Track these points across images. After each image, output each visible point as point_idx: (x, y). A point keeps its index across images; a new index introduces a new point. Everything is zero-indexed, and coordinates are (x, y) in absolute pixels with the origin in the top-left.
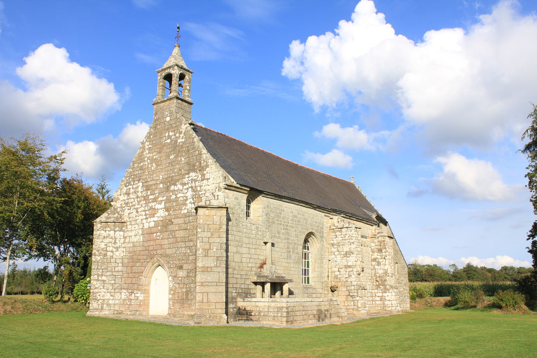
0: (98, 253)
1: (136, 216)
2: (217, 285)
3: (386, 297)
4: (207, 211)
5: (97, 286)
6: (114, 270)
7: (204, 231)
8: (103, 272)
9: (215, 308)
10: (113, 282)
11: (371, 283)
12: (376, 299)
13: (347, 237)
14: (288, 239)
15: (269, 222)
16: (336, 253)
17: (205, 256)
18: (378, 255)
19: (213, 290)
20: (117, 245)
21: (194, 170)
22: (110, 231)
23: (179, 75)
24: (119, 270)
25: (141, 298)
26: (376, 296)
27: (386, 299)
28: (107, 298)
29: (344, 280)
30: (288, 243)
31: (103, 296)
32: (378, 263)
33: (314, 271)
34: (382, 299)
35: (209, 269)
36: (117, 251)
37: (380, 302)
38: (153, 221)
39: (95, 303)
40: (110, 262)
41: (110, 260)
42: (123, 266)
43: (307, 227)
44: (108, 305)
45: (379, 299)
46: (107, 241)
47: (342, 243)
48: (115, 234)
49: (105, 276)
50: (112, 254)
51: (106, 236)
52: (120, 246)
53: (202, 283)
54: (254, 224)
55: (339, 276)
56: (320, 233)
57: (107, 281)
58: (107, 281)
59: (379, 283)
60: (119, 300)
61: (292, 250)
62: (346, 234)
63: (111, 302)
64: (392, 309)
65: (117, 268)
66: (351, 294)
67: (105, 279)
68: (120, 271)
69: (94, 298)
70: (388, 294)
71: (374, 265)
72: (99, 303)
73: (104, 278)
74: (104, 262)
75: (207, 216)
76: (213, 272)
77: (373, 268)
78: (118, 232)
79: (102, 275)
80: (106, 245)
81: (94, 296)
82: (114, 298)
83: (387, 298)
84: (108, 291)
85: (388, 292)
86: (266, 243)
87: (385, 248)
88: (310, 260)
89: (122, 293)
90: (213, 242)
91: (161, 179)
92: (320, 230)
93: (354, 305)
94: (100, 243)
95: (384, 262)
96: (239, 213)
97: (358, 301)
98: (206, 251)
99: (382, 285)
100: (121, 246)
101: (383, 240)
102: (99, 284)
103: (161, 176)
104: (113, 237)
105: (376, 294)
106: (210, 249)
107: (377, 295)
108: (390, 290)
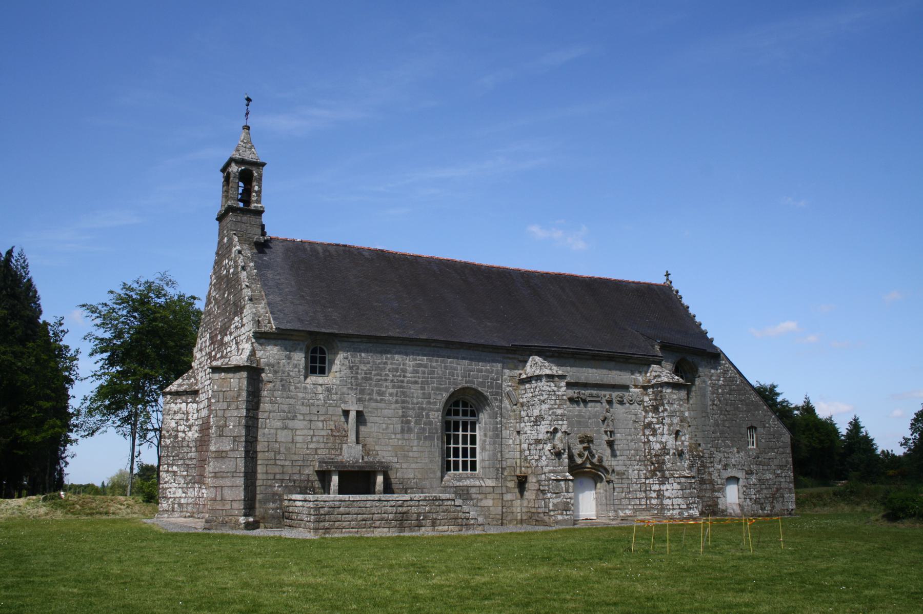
2: (233, 477)
3: (665, 492)
5: (167, 480)
7: (219, 402)
8: (173, 460)
9: (231, 509)
10: (185, 473)
12: (651, 495)
14: (403, 402)
15: (356, 378)
16: (526, 418)
17: (220, 436)
18: (653, 417)
19: (229, 484)
20: (190, 422)
22: (180, 403)
23: (237, 174)
24: (193, 457)
25: (205, 495)
26: (651, 490)
27: (665, 494)
28: (178, 496)
29: (535, 464)
32: (653, 432)
33: (483, 449)
34: (660, 495)
35: (224, 454)
36: (190, 430)
37: (656, 500)
40: (182, 446)
42: (196, 452)
43: (454, 379)
44: (180, 505)
45: (654, 495)
46: (177, 418)
49: (176, 465)
50: (184, 435)
53: (215, 473)
54: (321, 385)
55: (529, 458)
59: (655, 466)
60: (192, 498)
61: (413, 420)
62: (536, 387)
63: (183, 501)
64: (672, 515)
65: (190, 454)
66: (542, 488)
70: (667, 486)
71: (649, 435)
72: (170, 503)
73: (175, 468)
77: (646, 440)
79: (172, 465)
80: (177, 423)
83: (667, 494)
85: (667, 483)
86: (318, 412)
87: (663, 405)
88: (477, 433)
90: (229, 415)
92: (492, 383)
93: (545, 507)
95: (661, 429)
97: (549, 499)
99: (659, 471)
103: (219, 324)
107: (653, 489)
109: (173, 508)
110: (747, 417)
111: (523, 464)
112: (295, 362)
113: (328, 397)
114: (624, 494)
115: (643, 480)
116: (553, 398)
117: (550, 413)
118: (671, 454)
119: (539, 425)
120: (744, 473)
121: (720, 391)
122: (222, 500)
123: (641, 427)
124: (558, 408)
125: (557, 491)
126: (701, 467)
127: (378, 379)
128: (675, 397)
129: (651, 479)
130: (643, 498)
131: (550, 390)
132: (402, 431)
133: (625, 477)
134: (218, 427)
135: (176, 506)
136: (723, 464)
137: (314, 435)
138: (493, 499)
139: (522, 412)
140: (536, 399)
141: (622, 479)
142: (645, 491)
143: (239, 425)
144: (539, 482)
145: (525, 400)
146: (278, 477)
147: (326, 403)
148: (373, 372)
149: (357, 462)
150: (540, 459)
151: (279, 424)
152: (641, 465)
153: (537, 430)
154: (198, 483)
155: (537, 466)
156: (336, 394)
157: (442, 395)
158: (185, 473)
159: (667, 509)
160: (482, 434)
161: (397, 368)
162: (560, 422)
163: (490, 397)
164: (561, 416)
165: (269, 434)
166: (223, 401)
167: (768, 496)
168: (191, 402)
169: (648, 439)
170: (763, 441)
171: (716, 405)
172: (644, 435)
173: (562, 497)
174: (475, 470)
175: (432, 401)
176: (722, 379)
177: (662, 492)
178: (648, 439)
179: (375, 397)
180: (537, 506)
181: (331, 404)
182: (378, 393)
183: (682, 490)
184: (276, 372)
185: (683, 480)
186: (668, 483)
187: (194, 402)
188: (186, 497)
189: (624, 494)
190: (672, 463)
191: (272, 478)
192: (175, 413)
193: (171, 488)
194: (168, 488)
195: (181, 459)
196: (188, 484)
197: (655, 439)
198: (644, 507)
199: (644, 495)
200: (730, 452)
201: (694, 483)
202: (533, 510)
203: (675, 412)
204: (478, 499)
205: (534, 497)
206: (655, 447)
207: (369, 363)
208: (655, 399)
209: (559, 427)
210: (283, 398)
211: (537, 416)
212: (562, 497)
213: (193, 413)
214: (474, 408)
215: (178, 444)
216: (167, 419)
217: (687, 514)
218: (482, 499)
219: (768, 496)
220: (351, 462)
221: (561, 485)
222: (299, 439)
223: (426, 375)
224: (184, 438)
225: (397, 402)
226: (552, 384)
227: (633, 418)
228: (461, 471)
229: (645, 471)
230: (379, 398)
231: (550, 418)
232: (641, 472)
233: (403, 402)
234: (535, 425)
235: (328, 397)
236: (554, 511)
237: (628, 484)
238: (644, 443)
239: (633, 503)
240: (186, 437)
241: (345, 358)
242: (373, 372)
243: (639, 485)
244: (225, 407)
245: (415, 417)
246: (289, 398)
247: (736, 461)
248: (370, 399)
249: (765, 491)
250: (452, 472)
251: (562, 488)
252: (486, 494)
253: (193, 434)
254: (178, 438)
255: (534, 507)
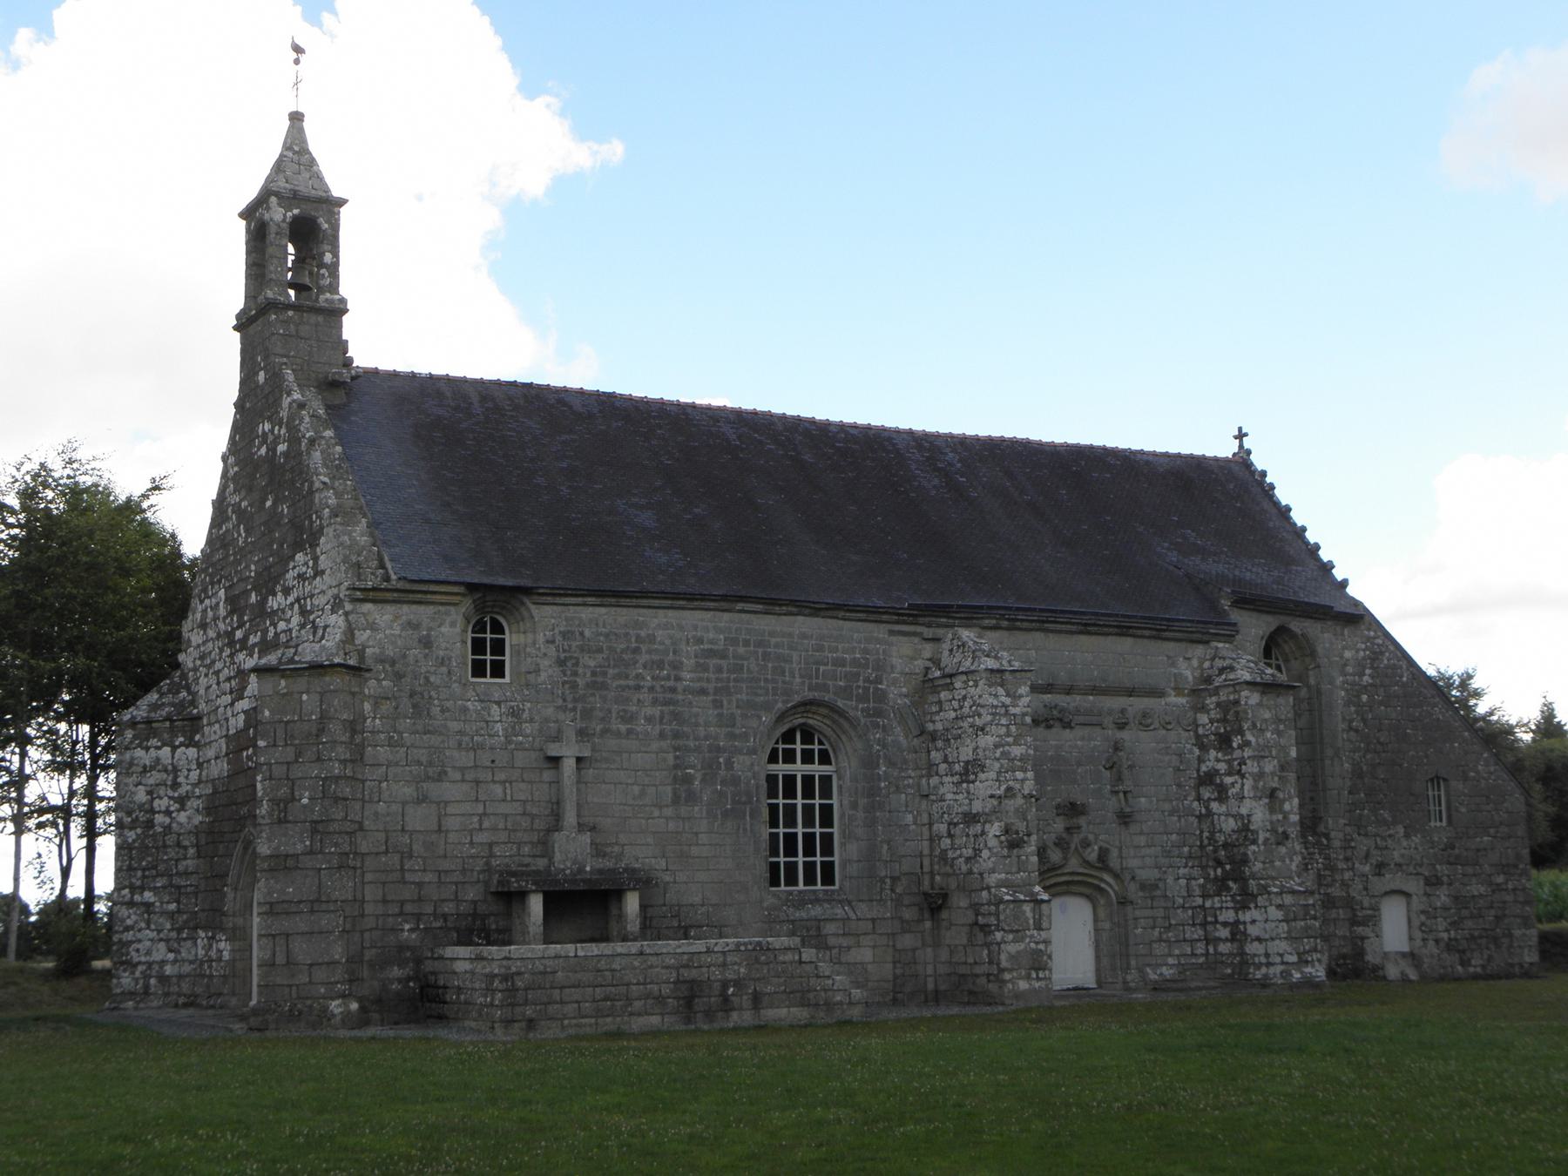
0: (129, 819)
1: (217, 696)
2: (312, 911)
4: (283, 683)
5: (129, 922)
6: (174, 871)
7: (275, 745)
8: (144, 877)
9: (310, 982)
10: (173, 906)
11: (1196, 872)
12: (1217, 934)
13: (968, 709)
14: (676, 735)
15: (574, 686)
16: (943, 766)
17: (280, 822)
18: (1218, 760)
19: (303, 927)
20: (183, 790)
21: (302, 549)
23: (284, 225)
24: (190, 869)
25: (226, 955)
26: (1216, 922)
27: (1249, 932)
29: (964, 868)
30: (676, 749)
31: (148, 953)
33: (847, 836)
34: (1238, 933)
35: (290, 863)
36: (182, 808)
37: (1229, 944)
38: (243, 711)
39: (127, 974)
40: (165, 846)
41: (164, 841)
42: (199, 857)
43: (784, 682)
44: (163, 979)
45: (1224, 933)
46: (151, 781)
47: (955, 732)
48: (173, 758)
49: (150, 889)
50: (167, 820)
51: (148, 764)
52: (190, 795)
53: (271, 904)
55: (950, 854)
56: (863, 698)
57: (158, 904)
58: (158, 904)
59: (1224, 870)
60: (191, 962)
61: (699, 776)
62: (964, 698)
63: (168, 970)
64: (1266, 976)
65: (184, 863)
66: (981, 920)
67: (152, 900)
68: (192, 873)
69: (124, 958)
70: (1252, 914)
71: (1209, 799)
72: (138, 974)
73: (148, 896)
74: (147, 847)
75: (285, 695)
76: (301, 869)
77: (1203, 811)
78: (183, 748)
79: (142, 889)
80: (150, 793)
81: (123, 955)
82: (179, 957)
83: (1253, 931)
84: (161, 935)
86: (493, 761)
87: (1241, 732)
88: (835, 801)
89: (199, 941)
90: (300, 775)
91: (253, 574)
92: (866, 689)
93: (991, 962)
94: (134, 789)
95: (1238, 786)
96: (428, 672)
97: (999, 944)
98: (282, 805)
99: (1235, 881)
100: (193, 792)
101: (1232, 697)
102: (135, 913)
103: (253, 567)
104: (170, 768)
105: (1218, 913)
106: (293, 799)
107: (1221, 919)
108: (1259, 898)
109: (147, 987)
110: (1427, 756)
111: (936, 867)
112: (441, 653)
113: (513, 728)
114: (1156, 932)
115: (1199, 901)
116: (1004, 721)
117: (998, 755)
118: (1260, 842)
119: (973, 782)
120: (1422, 883)
121: (1364, 698)
122: (288, 963)
123: (1192, 782)
124: (1014, 744)
125: (1016, 927)
126: (1324, 870)
127: (620, 686)
128: (1267, 715)
129: (1216, 899)
130: (1200, 940)
131: (995, 703)
132: (676, 800)
133: (1158, 893)
134: (275, 802)
135: (153, 981)
136: (1374, 862)
137: (485, 814)
138: (874, 947)
139: (933, 753)
140: (965, 725)
141: (1152, 898)
142: (1204, 924)
143: (324, 797)
144: (976, 908)
145: (939, 726)
146: (409, 908)
147: (510, 742)
148: (611, 671)
149: (581, 870)
150: (976, 855)
151: (408, 791)
152: (1192, 867)
153: (968, 793)
154: (205, 928)
155: (970, 872)
156: (531, 720)
157: (760, 718)
158: (173, 906)
159: (1254, 964)
160: (845, 802)
161: (662, 662)
162: (1019, 775)
163: (863, 721)
164: (1020, 760)
165: (388, 814)
166: (286, 745)
167: (1476, 933)
168: (182, 744)
169: (1207, 808)
170: (1463, 810)
171: (1357, 731)
172: (1199, 799)
173: (1028, 940)
174: (833, 883)
175: (737, 731)
176: (1368, 671)
177: (1241, 927)
178: (1207, 808)
179: (614, 727)
180: (971, 960)
181: (521, 743)
182: (622, 717)
183: (1286, 921)
184: (399, 676)
185: (1288, 899)
186: (1256, 907)
187: (190, 743)
188: (175, 961)
189: (1156, 932)
190: (1264, 863)
191: (397, 910)
192: (145, 770)
193: (140, 941)
194: (132, 942)
195: (162, 876)
196: (179, 930)
197: (1224, 809)
198: (1202, 960)
199: (1201, 932)
200: (1390, 836)
201: (1313, 905)
202: (963, 970)
203: (1267, 747)
204: (840, 947)
205: (965, 941)
206: (1223, 825)
207: (600, 650)
208: (1224, 720)
209: (1018, 786)
210: (417, 732)
211: (967, 763)
212: (1028, 940)
213: (189, 770)
214: (827, 746)
215: (155, 841)
216: (126, 785)
217: (1299, 976)
218: (849, 948)
219: (1476, 933)
220: (568, 872)
221: (1024, 913)
222: (452, 823)
223: (725, 675)
224: (169, 827)
225: (662, 736)
226: (1001, 691)
227: (1175, 760)
228: (801, 886)
229: (1202, 881)
230: (623, 728)
231: (997, 765)
232: (1193, 882)
233: (676, 735)
234: (963, 782)
235: (513, 728)
236: (1010, 970)
237: (1165, 908)
238: (1200, 817)
239: (1177, 952)
240: (174, 825)
241: (548, 642)
242: (611, 671)
243: (1190, 912)
244: (291, 757)
245: (703, 768)
246: (429, 732)
247: (1402, 856)
248: (605, 731)
249: (1469, 924)
250: (783, 887)
251: (1027, 920)
252: (858, 935)
253: (189, 818)
254: (153, 826)
255: (965, 963)
